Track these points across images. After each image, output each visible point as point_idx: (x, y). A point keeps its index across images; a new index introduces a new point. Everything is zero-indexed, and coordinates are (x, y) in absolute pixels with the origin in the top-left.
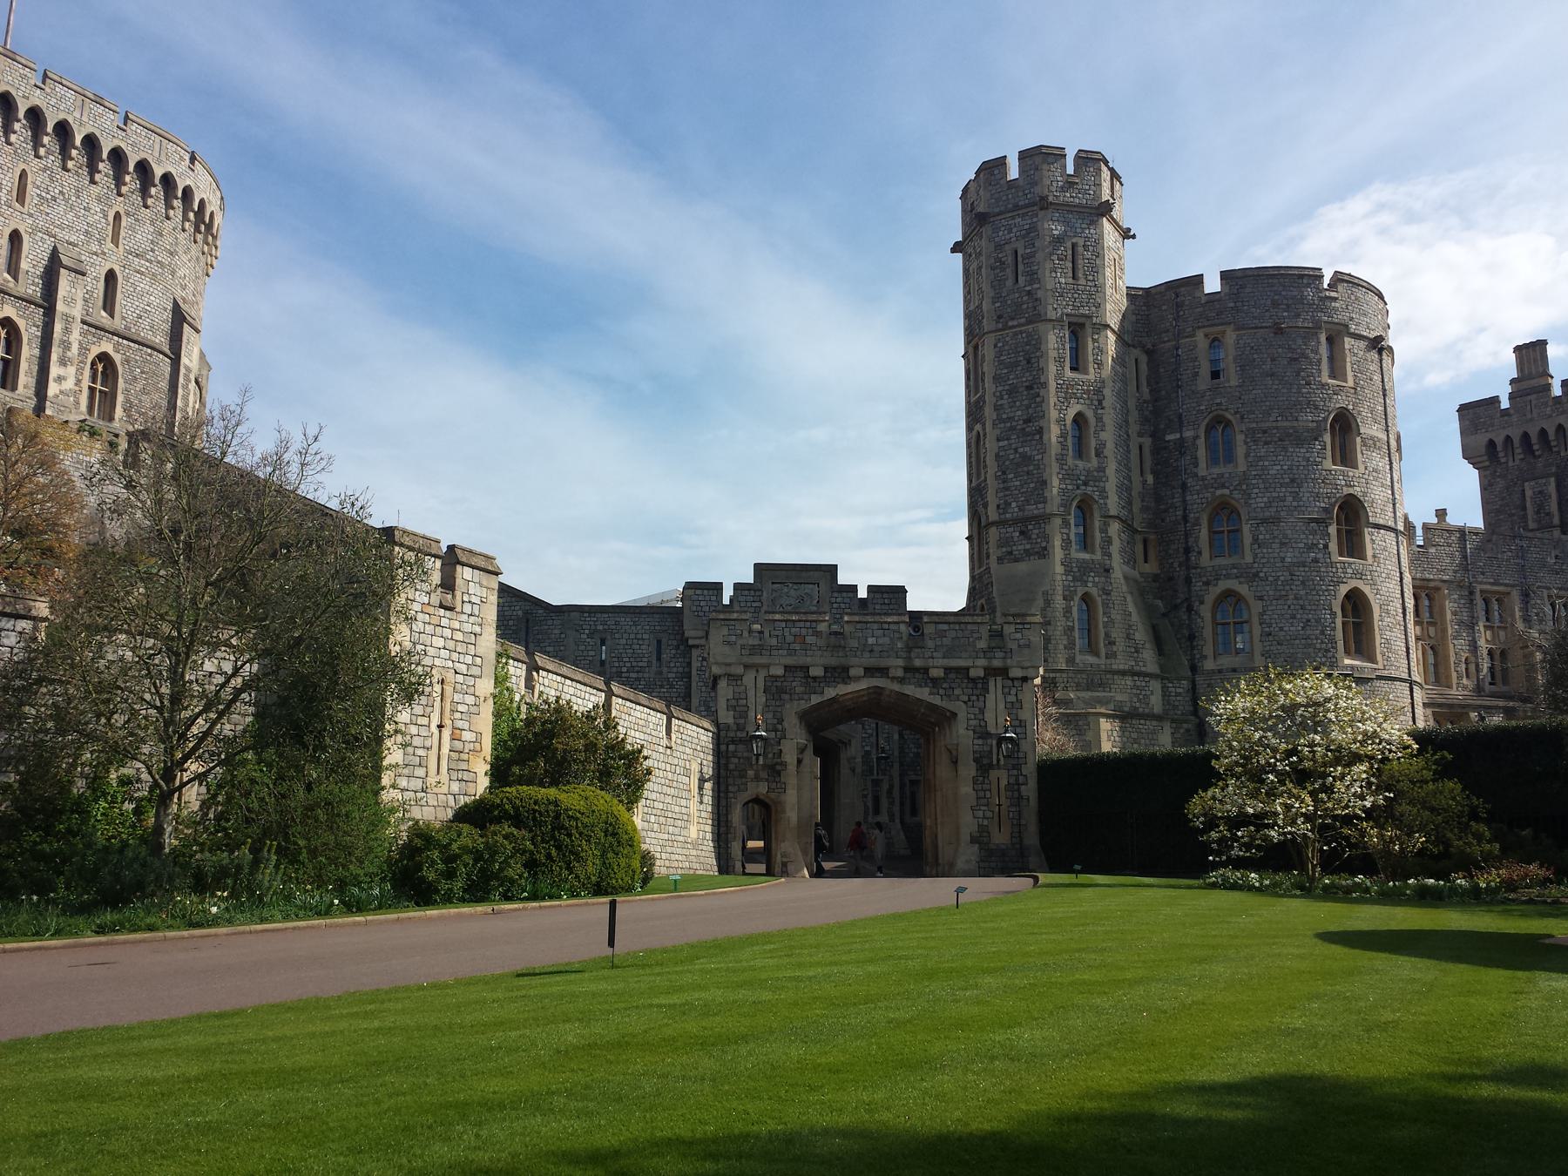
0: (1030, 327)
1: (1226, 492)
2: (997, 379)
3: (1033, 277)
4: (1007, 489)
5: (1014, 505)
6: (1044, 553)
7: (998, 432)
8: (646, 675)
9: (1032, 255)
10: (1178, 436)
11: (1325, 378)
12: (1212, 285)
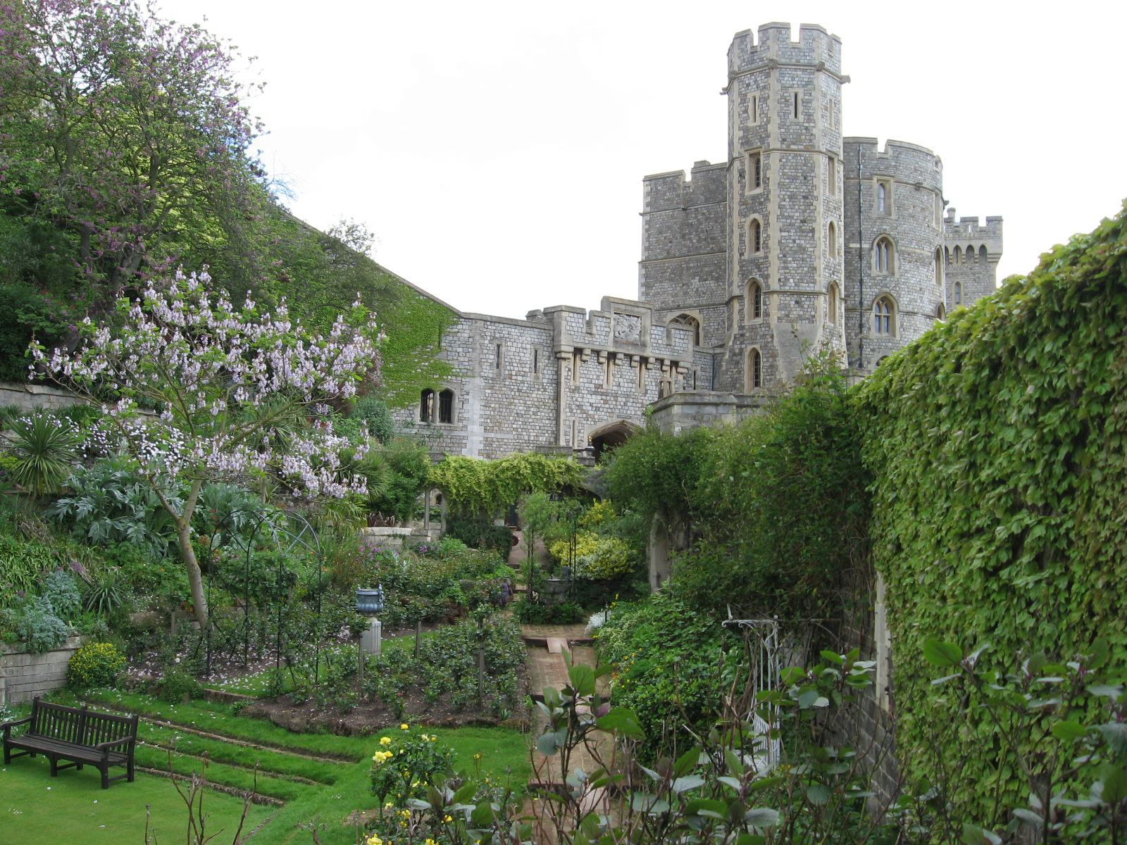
0: (807, 154)
1: (887, 290)
2: (780, 185)
3: (809, 118)
4: (787, 268)
5: (791, 281)
6: (812, 319)
7: (781, 225)
8: (528, 379)
9: (809, 102)
10: (858, 246)
11: (934, 225)
12: (881, 148)
